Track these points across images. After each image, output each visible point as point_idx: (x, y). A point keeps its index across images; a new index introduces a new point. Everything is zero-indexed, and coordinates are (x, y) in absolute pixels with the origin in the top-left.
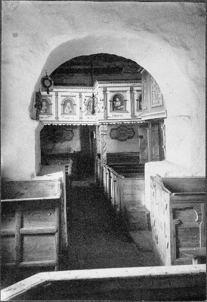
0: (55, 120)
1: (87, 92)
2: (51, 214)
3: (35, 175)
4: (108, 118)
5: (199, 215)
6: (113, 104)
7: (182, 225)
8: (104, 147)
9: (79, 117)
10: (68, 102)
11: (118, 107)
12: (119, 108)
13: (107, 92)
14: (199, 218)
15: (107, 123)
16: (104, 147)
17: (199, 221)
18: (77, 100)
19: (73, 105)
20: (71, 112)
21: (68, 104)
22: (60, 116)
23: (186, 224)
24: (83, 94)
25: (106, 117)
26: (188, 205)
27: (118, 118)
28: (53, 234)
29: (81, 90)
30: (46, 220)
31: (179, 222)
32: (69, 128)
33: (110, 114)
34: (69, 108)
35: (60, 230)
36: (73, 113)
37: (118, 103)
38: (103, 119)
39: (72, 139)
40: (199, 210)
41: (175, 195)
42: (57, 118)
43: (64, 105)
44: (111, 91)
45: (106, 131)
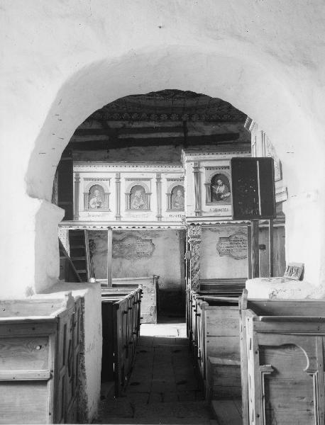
0: (115, 219)
1: (168, 172)
2: (41, 347)
3: (34, 291)
4: (204, 215)
5: (310, 358)
6: (212, 189)
7: (278, 377)
10: (137, 190)
11: (220, 195)
12: (222, 196)
13: (201, 170)
14: (310, 364)
15: (200, 223)
17: (311, 371)
18: (152, 187)
19: (146, 195)
21: (138, 193)
22: (123, 213)
23: (286, 374)
24: (163, 176)
25: (199, 212)
26: (286, 339)
27: (222, 214)
28: (43, 383)
29: (159, 169)
30: (34, 358)
31: (272, 370)
32: (149, 236)
33: (205, 208)
34: (139, 199)
35: (56, 375)
36: (145, 207)
38: (194, 215)
39: (151, 253)
40: (310, 349)
41: (263, 320)
42: (118, 217)
43: (130, 195)
44: (207, 168)
45: (199, 237)
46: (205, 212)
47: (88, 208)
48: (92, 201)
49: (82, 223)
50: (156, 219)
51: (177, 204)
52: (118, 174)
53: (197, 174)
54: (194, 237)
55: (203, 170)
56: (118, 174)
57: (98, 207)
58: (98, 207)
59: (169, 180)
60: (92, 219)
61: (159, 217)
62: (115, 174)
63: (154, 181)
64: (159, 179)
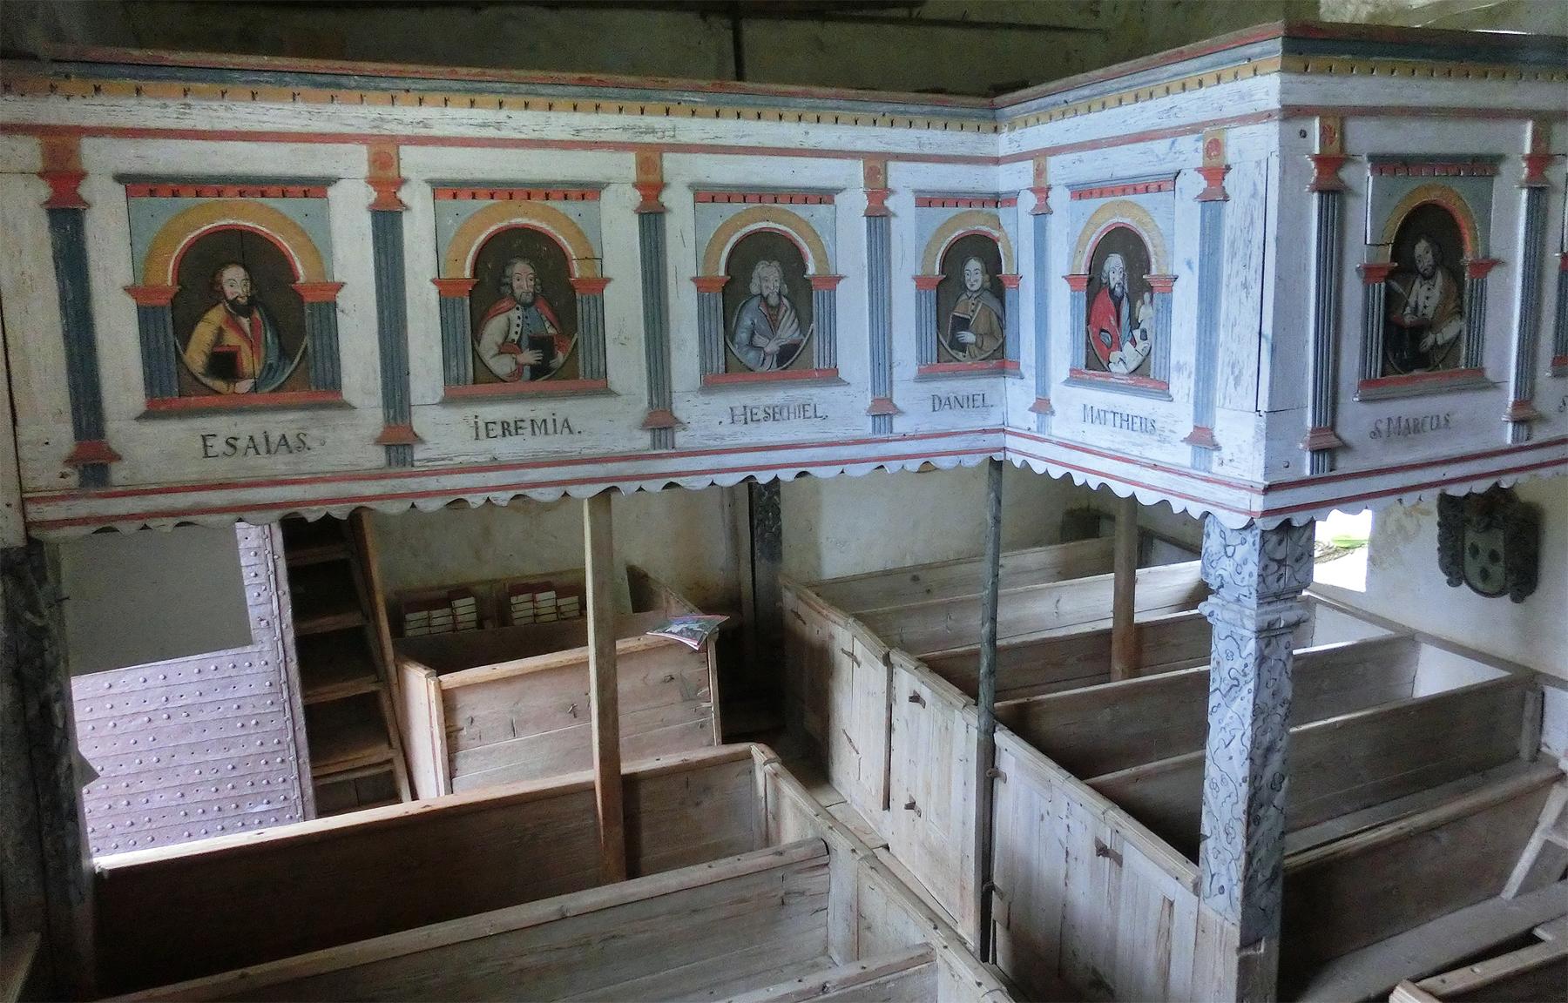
0: (643, 441)
8: (1270, 749)
9: (868, 400)
11: (1423, 327)
12: (1429, 340)
13: (1348, 174)
16: (1270, 749)
18: (841, 239)
19: (805, 292)
20: (786, 355)
21: (767, 278)
24: (901, 176)
33: (1357, 417)
37: (1425, 296)
43: (729, 293)
46: (1346, 447)
47: (470, 379)
48: (494, 329)
49: (432, 484)
50: (866, 427)
51: (968, 337)
52: (650, 158)
53: (1333, 194)
54: (1278, 597)
55: (1363, 180)
56: (650, 158)
57: (539, 371)
58: (539, 371)
59: (926, 200)
60: (506, 448)
61: (884, 410)
62: (631, 158)
63: (854, 203)
64: (878, 192)
